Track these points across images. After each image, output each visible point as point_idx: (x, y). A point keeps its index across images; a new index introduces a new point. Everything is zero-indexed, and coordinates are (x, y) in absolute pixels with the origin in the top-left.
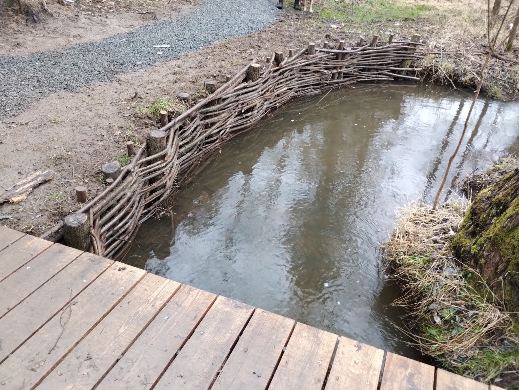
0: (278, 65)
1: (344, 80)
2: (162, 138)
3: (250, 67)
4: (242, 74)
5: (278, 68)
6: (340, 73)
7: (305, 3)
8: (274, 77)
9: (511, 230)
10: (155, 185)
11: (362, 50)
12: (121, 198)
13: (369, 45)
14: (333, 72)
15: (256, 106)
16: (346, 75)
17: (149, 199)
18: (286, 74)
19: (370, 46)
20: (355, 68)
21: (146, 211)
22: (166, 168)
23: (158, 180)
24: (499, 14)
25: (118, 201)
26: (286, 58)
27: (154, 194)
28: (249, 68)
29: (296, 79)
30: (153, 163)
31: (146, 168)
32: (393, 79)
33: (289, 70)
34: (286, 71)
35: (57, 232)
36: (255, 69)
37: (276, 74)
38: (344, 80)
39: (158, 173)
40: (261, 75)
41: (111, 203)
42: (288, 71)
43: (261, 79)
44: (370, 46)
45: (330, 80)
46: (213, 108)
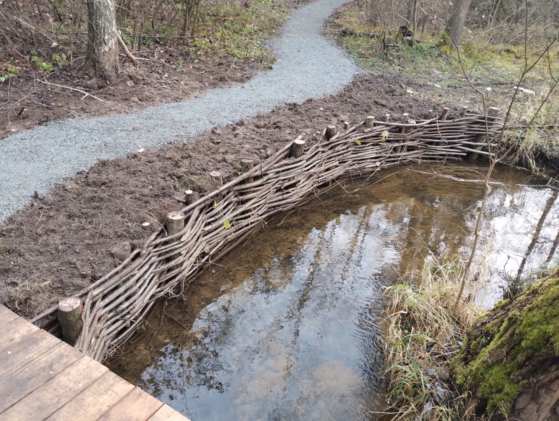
0: (328, 140)
1: (406, 153)
2: (179, 221)
3: (294, 144)
4: (286, 150)
5: (328, 142)
6: (403, 147)
7: (2, 267)
8: (323, 152)
9: (491, 366)
10: (172, 263)
11: (430, 123)
12: (128, 279)
13: (438, 117)
14: (394, 146)
15: (299, 181)
16: (410, 149)
17: (164, 278)
18: (336, 149)
19: (439, 119)
20: (420, 141)
21: (159, 289)
22: (183, 248)
23: (175, 259)
24: (314, 228)
25: (124, 282)
26: (338, 133)
27: (171, 273)
28: (292, 146)
29: (351, 152)
30: (171, 243)
31: (161, 249)
32: (465, 154)
33: (341, 144)
34: (338, 145)
35: (46, 317)
36: (298, 146)
37: (326, 149)
38: (406, 153)
39: (176, 252)
40: (305, 151)
41: (117, 284)
42: (341, 145)
43: (304, 156)
44: (439, 119)
45: (391, 153)
46: (248, 185)
